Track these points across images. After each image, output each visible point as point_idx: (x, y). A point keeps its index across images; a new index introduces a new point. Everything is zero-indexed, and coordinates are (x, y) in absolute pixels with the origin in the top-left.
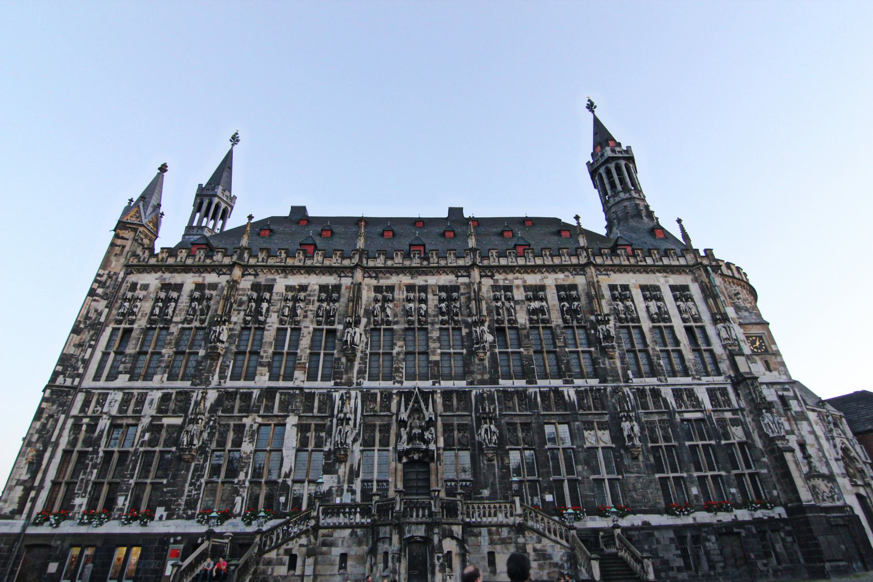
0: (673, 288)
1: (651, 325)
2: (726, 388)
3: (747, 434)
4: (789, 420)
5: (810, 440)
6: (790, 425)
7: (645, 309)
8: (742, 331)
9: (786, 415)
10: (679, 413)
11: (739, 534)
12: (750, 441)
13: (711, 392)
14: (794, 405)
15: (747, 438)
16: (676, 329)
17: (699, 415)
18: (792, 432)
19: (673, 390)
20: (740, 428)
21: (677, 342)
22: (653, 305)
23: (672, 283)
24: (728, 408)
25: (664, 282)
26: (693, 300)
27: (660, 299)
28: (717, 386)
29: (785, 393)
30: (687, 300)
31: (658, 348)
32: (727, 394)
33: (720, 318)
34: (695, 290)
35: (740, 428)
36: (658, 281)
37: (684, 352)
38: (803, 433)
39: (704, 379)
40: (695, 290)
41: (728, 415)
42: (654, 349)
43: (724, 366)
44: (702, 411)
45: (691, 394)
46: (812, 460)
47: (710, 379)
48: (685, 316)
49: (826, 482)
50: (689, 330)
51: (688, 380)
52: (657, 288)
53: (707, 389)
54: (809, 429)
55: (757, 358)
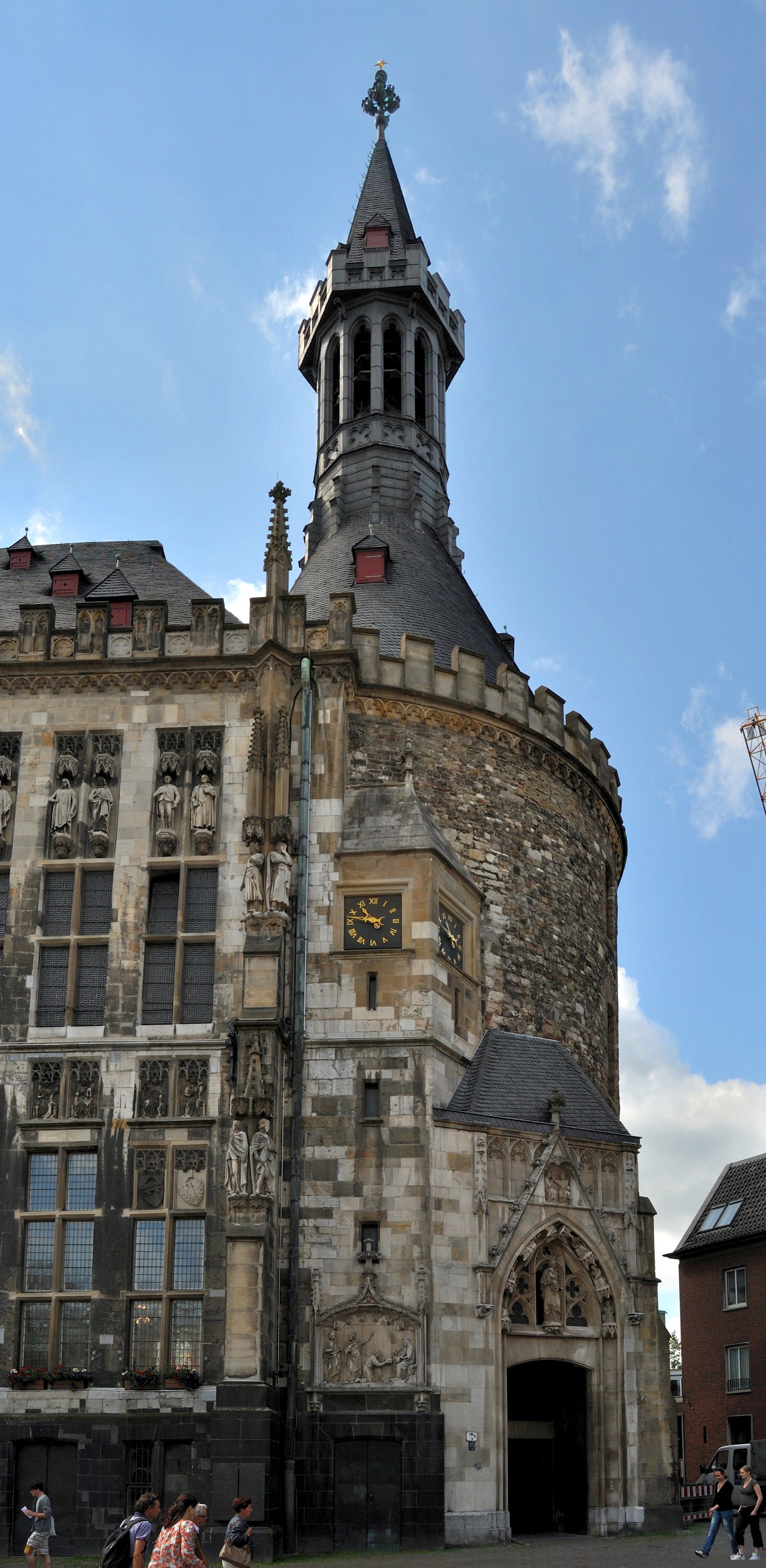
0: (168, 739)
1: (42, 862)
2: (205, 1062)
3: (213, 1192)
4: (359, 1155)
5: (402, 1210)
6: (358, 1167)
7: (38, 815)
8: (335, 877)
9: (360, 1137)
10: (25, 1128)
11: (74, 1444)
12: (211, 1213)
13: (152, 1076)
14: (400, 1112)
15: (209, 1203)
16: (118, 876)
17: (84, 1136)
18: (356, 1189)
19: (35, 1065)
20: (203, 1175)
21: (109, 916)
22: (72, 802)
23: (171, 717)
24: (187, 1117)
25: (138, 721)
26: (214, 775)
27: (109, 779)
28: (175, 1053)
29: (387, 1074)
30: (196, 781)
31: (36, 937)
32: (205, 1075)
33: (275, 835)
34: (238, 742)
35: (203, 1175)
36: (127, 715)
37: (115, 948)
38: (387, 1193)
39: (144, 1032)
40: (238, 742)
41: (177, 1138)
42: (21, 942)
43: (225, 993)
44: (98, 1126)
45: (87, 1076)
46: (381, 1269)
47: (164, 1031)
48: (163, 832)
49: (396, 1326)
50: (162, 880)
51: (95, 1033)
52: (111, 742)
53: (143, 1064)
54: (414, 1180)
55: (347, 965)
